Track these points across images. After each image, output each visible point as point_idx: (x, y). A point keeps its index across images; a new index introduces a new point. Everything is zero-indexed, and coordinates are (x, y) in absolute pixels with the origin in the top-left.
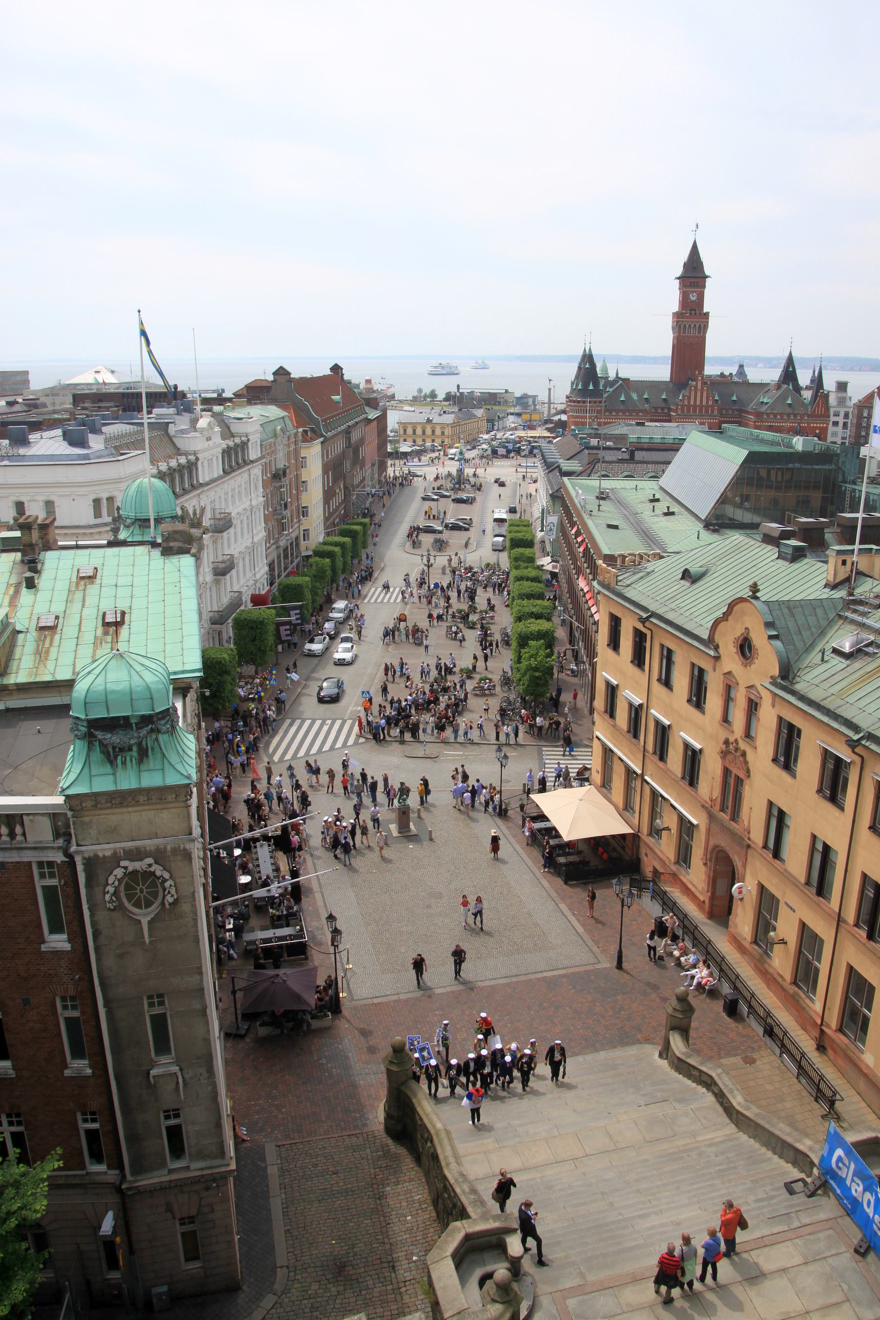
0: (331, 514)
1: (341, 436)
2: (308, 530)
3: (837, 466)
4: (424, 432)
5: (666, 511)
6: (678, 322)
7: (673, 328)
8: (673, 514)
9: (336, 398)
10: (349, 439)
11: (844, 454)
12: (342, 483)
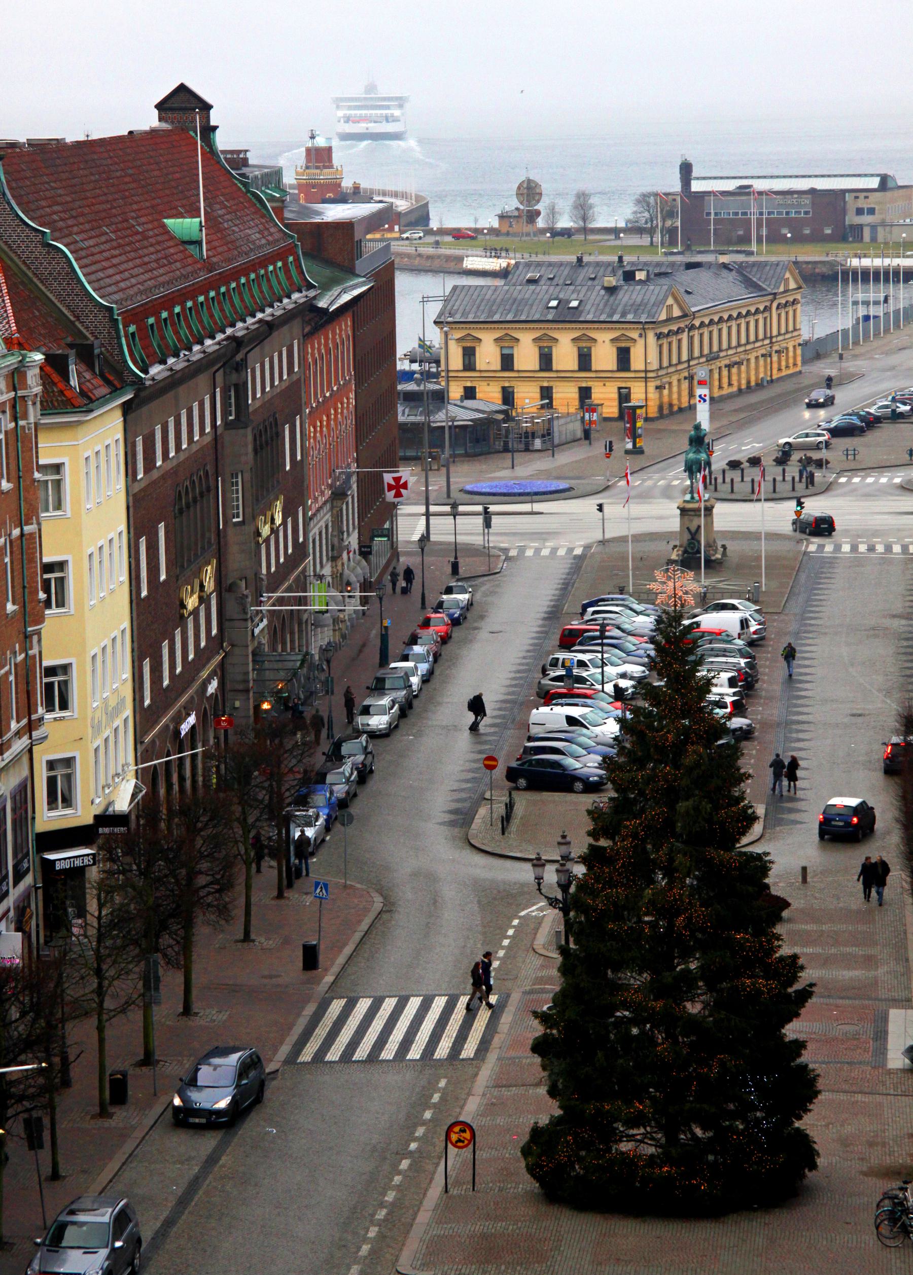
0: (163, 698)
1: (203, 380)
2: (68, 762)
4: (546, 361)
9: (185, 226)
10: (241, 390)
12: (209, 571)
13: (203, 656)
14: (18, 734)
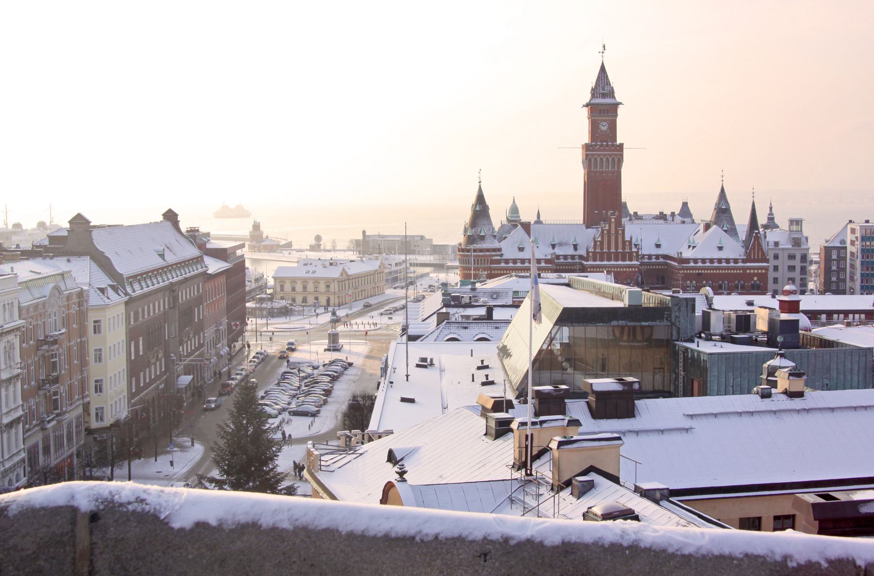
0: (139, 390)
1: (160, 295)
2: (102, 408)
3: (670, 321)
5: (484, 380)
6: (587, 156)
7: (583, 163)
8: (492, 383)
11: (676, 308)
13: (157, 378)
14: (78, 400)
